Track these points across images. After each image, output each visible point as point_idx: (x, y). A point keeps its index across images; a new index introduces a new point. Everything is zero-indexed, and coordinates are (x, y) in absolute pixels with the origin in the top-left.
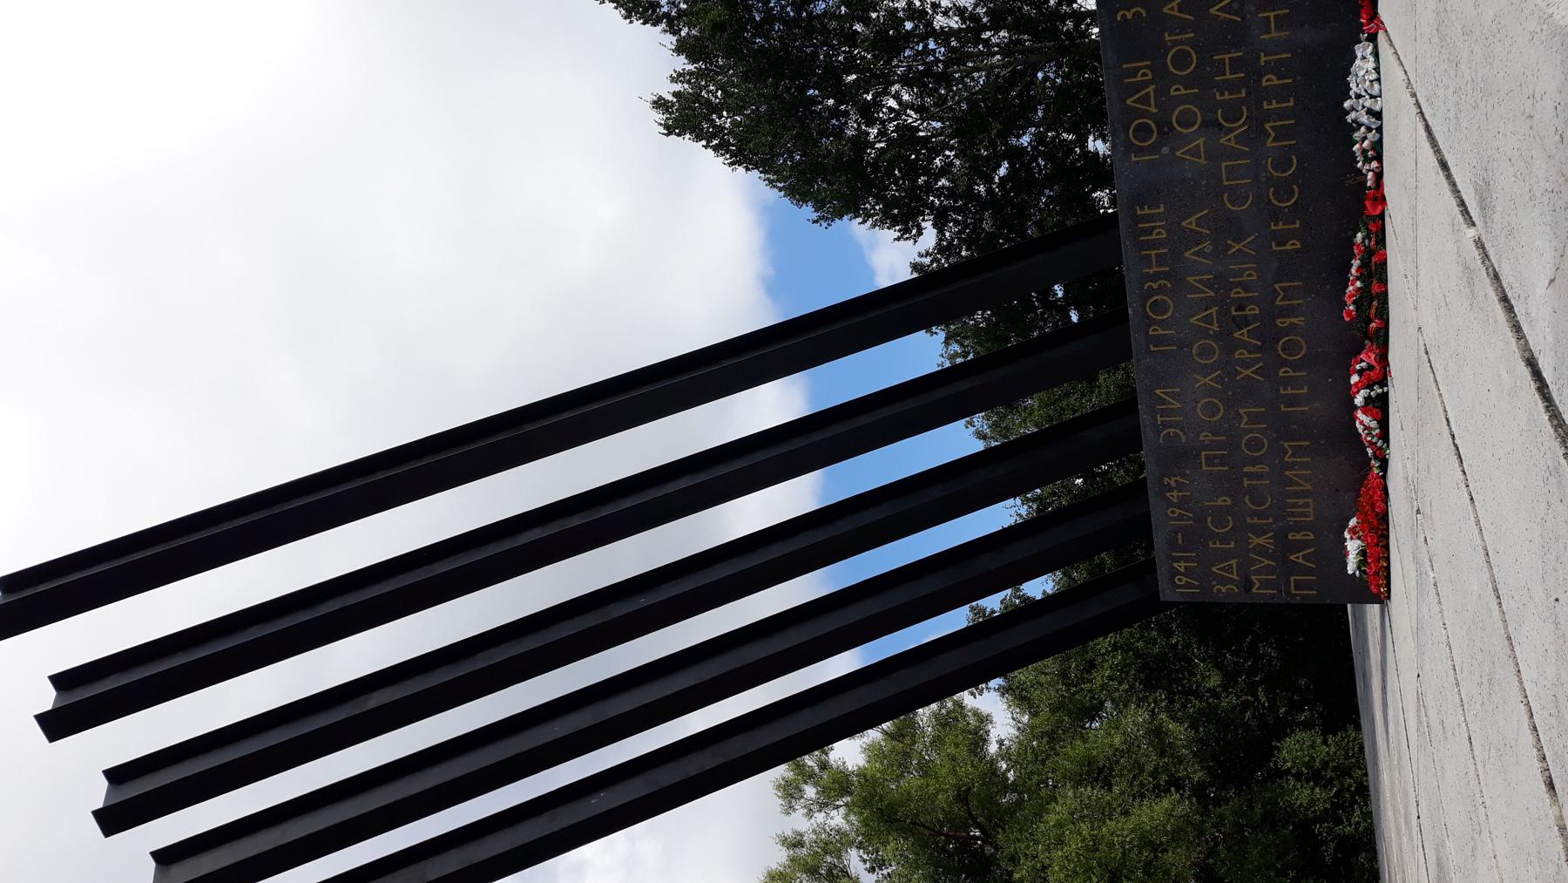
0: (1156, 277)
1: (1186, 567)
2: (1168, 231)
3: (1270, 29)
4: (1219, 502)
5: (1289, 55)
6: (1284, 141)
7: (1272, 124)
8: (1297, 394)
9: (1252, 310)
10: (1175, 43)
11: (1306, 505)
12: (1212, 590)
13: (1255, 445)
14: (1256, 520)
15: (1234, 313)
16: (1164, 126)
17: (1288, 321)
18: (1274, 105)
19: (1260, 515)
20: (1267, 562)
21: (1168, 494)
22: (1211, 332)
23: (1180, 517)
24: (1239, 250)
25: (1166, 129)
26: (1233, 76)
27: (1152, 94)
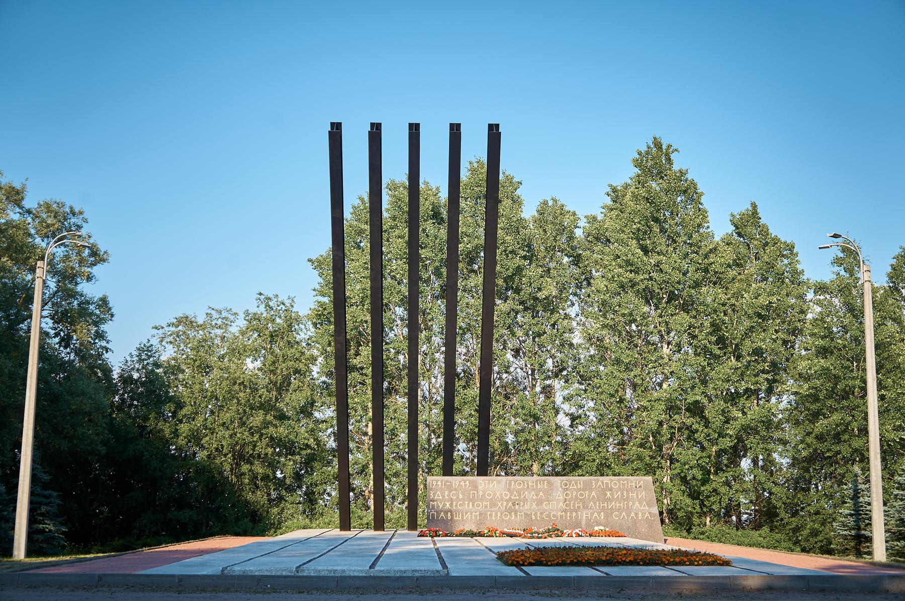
0: (528, 484)
9: (517, 507)
19: (456, 505)
20: (441, 507)
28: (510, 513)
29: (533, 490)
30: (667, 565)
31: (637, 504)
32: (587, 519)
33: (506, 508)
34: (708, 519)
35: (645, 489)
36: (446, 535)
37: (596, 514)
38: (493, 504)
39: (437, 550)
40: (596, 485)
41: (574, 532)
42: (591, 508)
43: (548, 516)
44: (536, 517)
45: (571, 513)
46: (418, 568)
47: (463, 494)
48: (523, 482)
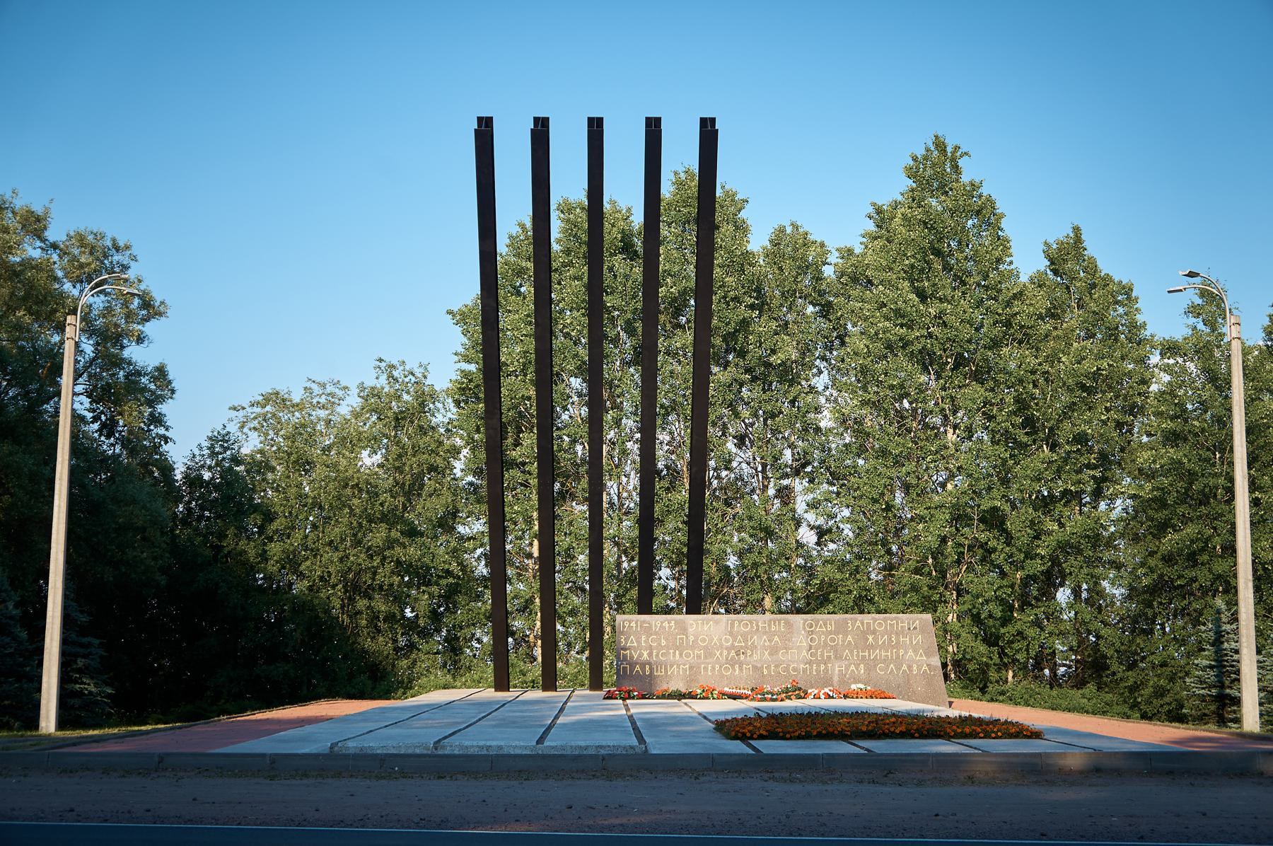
0: (757, 625)
9: (742, 657)
17: (737, 669)
19: (657, 655)
29: (765, 633)
30: (952, 737)
31: (911, 653)
32: (841, 674)
34: (1011, 674)
35: (923, 631)
36: (643, 697)
37: (853, 667)
38: (709, 653)
39: (631, 717)
41: (823, 692)
43: (786, 670)
45: (818, 666)
46: (604, 743)
47: (666, 640)
48: (750, 622)
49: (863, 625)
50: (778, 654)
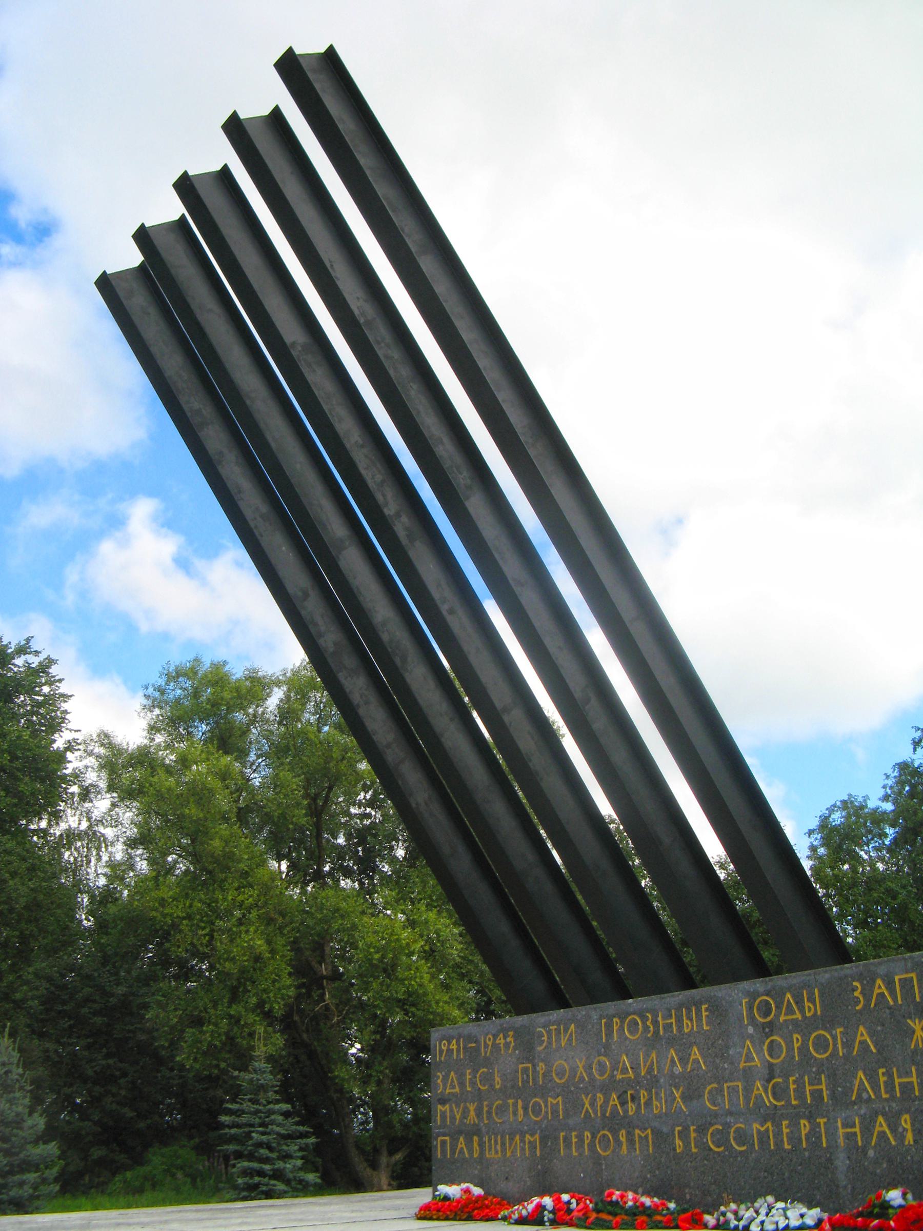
1: (453, 1049)
2: (689, 1034)
3: (847, 1127)
4: (497, 1079)
5: (824, 1145)
6: (758, 1139)
7: (771, 1128)
8: (571, 1146)
10: (834, 1038)
11: (497, 1152)
12: (439, 1071)
13: (537, 1110)
14: (485, 1109)
15: (629, 1092)
16: (769, 1028)
18: (785, 1131)
19: (489, 1113)
21: (501, 1035)
22: (615, 1073)
23: (486, 1046)
24: (675, 1097)
25: (767, 1030)
26: (808, 1093)
27: (794, 1017)
28: (615, 1133)
32: (856, 1151)
33: (604, 1115)
37: (881, 1124)
40: (867, 994)
42: (859, 1096)
44: (687, 1145)
45: (794, 1124)
49: (893, 992)
50: (701, 1096)
